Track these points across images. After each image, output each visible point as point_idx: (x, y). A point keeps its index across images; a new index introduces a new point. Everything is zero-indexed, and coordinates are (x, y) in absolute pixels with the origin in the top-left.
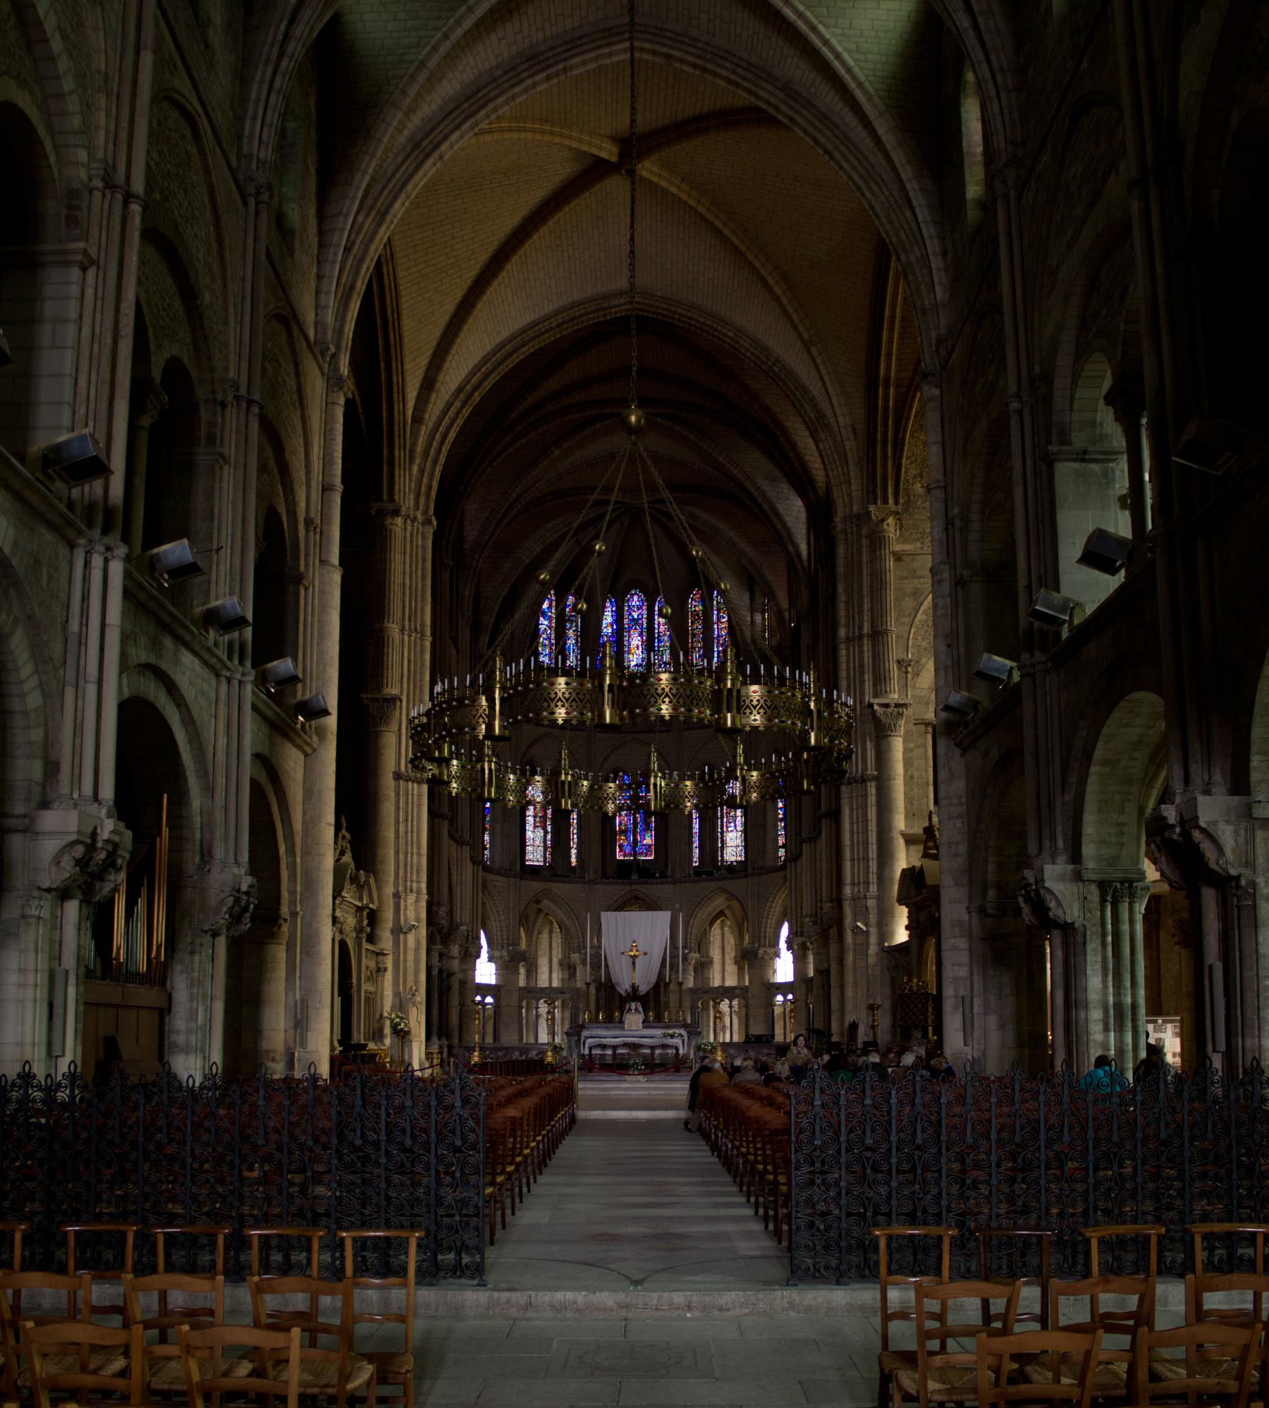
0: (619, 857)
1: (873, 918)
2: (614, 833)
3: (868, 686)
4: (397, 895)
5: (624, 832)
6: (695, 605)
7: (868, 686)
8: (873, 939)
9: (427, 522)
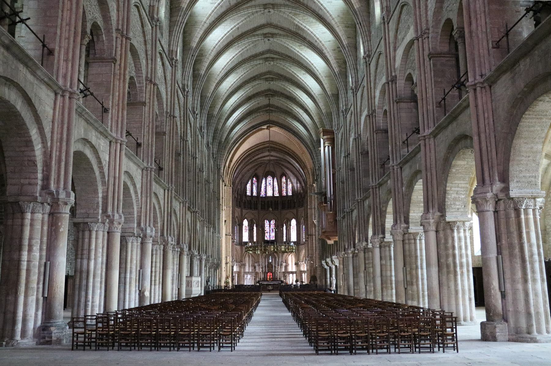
0: (266, 239)
1: (314, 261)
2: (265, 233)
3: (313, 218)
4: (226, 257)
5: (267, 233)
6: (284, 180)
7: (313, 218)
8: (314, 265)
9: (231, 186)
